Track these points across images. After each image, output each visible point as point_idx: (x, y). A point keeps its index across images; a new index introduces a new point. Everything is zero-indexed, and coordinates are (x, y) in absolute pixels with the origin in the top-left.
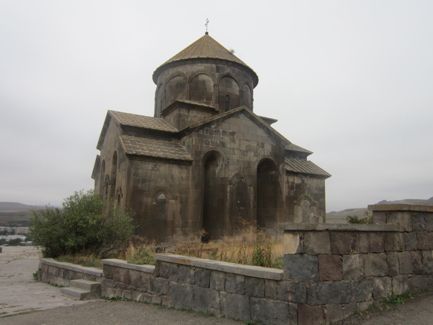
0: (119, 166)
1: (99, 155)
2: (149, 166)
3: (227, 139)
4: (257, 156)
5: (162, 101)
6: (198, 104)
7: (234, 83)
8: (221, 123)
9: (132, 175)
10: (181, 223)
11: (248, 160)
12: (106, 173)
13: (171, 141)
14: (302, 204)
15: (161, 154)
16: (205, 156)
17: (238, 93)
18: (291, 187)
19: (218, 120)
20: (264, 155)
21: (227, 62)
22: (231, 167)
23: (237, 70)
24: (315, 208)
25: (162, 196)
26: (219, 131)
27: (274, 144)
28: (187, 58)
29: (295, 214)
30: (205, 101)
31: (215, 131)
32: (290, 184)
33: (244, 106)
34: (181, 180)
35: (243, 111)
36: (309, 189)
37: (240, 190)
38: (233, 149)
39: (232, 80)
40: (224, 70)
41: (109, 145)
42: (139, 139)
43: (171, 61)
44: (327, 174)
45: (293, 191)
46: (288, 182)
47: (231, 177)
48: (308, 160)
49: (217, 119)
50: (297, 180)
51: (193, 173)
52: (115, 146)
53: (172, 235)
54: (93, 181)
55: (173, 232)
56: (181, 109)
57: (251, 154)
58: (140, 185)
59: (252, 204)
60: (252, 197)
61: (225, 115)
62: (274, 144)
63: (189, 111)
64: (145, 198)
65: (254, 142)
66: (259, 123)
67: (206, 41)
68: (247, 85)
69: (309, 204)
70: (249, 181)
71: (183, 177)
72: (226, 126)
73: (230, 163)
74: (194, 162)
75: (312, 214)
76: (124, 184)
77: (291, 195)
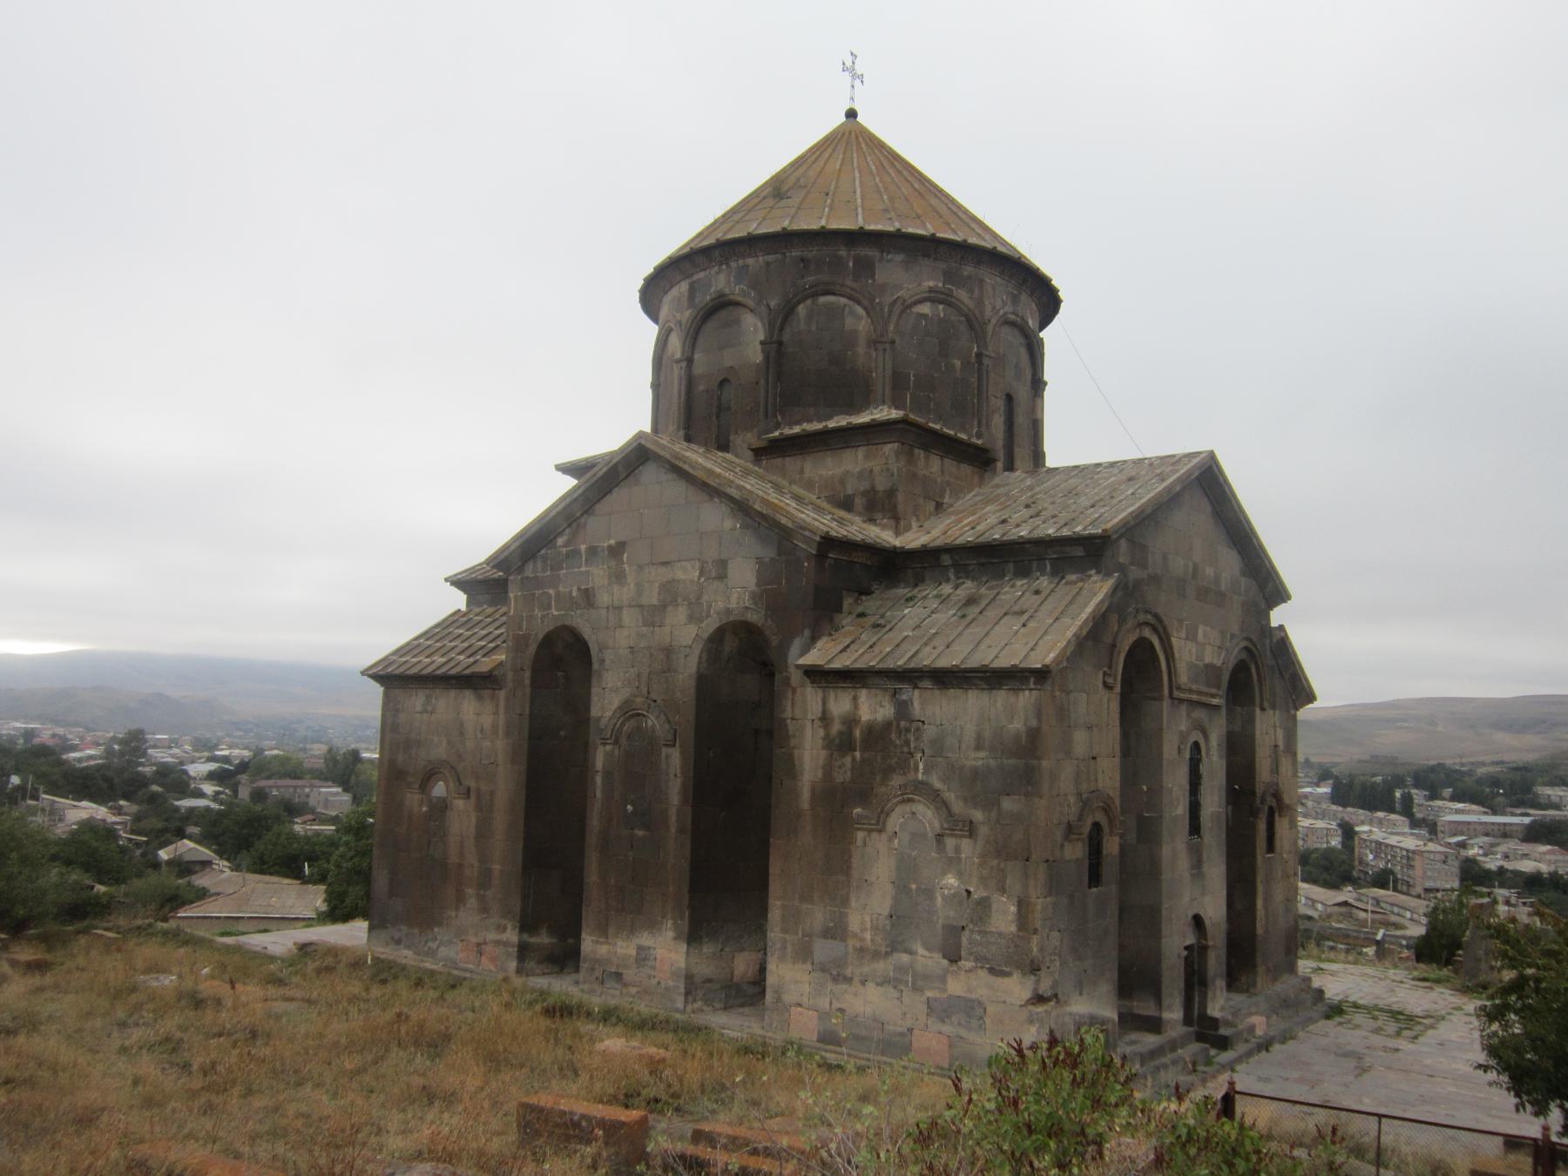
3: (598, 575)
14: (895, 821)
18: (841, 744)
20: (728, 611)
26: (577, 552)
29: (855, 874)
31: (567, 556)
32: (836, 727)
36: (938, 746)
38: (620, 608)
39: (742, 310)
45: (848, 760)
46: (825, 718)
50: (872, 708)
53: (457, 909)
55: (460, 899)
57: (678, 615)
58: (400, 758)
59: (673, 818)
62: (769, 553)
65: (688, 565)
69: (937, 824)
73: (608, 662)
75: (951, 880)
77: (839, 778)
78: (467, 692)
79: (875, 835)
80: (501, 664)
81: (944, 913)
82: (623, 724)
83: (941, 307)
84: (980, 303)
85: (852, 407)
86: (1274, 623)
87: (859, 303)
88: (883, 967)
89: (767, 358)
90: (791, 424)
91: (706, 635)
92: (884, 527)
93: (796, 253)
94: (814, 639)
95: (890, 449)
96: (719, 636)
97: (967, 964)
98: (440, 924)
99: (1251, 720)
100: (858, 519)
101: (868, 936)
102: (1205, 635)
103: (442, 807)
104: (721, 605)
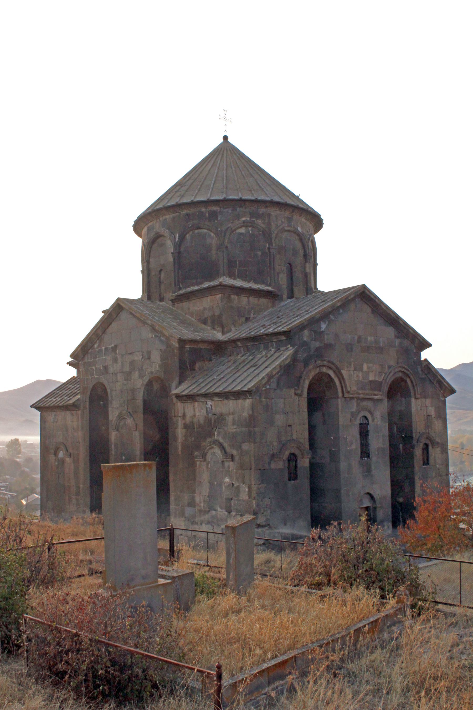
4: (143, 377)
8: (103, 336)
20: (152, 373)
24: (230, 465)
26: (101, 350)
27: (163, 347)
57: (136, 375)
62: (163, 347)
75: (227, 480)
80: (78, 400)
81: (226, 493)
82: (119, 423)
83: (250, 229)
84: (269, 225)
85: (211, 278)
86: (423, 358)
87: (212, 231)
88: (207, 517)
89: (174, 259)
90: (186, 287)
91: (145, 383)
92: (218, 331)
93: (184, 212)
94: (180, 383)
95: (219, 296)
96: (150, 384)
97: (233, 513)
99: (409, 404)
100: (209, 328)
101: (202, 505)
102: (368, 368)
103: (62, 462)
104: (149, 370)
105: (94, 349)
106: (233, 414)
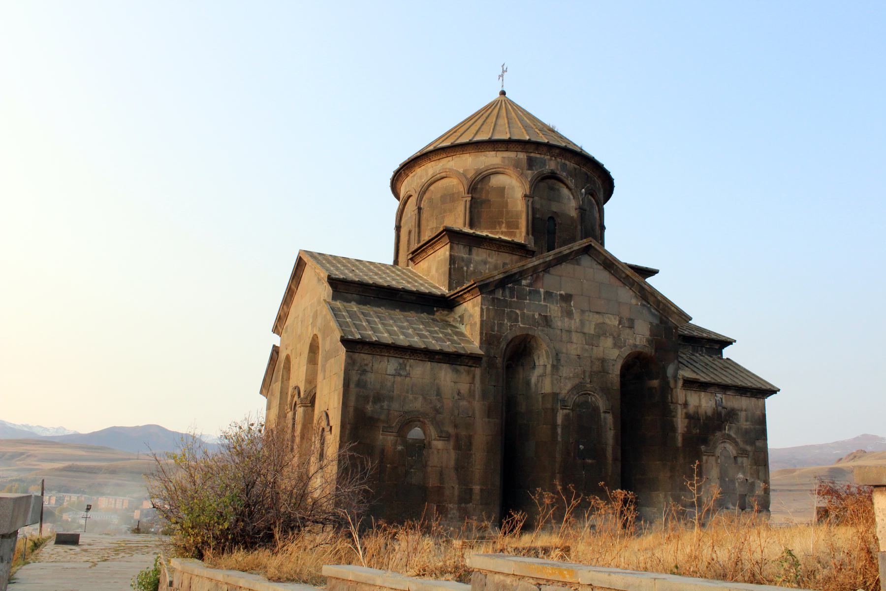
0: (324, 366)
1: (278, 345)
2: (390, 365)
3: (554, 310)
4: (620, 347)
5: (410, 232)
6: (490, 235)
7: (565, 191)
8: (541, 274)
9: (352, 386)
10: (456, 492)
11: (601, 355)
12: (292, 383)
13: (433, 313)
14: (718, 451)
15: (416, 341)
16: (508, 345)
17: (573, 213)
19: (535, 268)
20: (635, 346)
21: (549, 147)
22: (565, 371)
23: (570, 165)
25: (416, 433)
28: (465, 139)
30: (504, 230)
31: (530, 292)
33: (590, 239)
34: (456, 397)
35: (587, 250)
37: (584, 420)
38: (569, 331)
39: (561, 185)
40: (545, 164)
41: (300, 324)
42: (366, 309)
43: (431, 148)
44: (769, 387)
47: (564, 392)
48: (724, 357)
49: (535, 266)
51: (482, 382)
52: (313, 324)
54: (263, 401)
56: (455, 246)
58: (369, 408)
59: (609, 451)
60: (610, 435)
61: (551, 258)
62: (656, 321)
63: (470, 251)
64: (381, 437)
66: (624, 275)
67: (503, 105)
68: (592, 195)
70: (601, 403)
71: (462, 392)
72: (552, 282)
73: (562, 362)
74: (484, 359)
75: (741, 476)
76: (336, 405)
78: (445, 366)
79: (710, 458)
81: (739, 489)
98: (427, 530)
103: (421, 446)
104: (631, 342)
105: (521, 285)
106: (746, 410)
